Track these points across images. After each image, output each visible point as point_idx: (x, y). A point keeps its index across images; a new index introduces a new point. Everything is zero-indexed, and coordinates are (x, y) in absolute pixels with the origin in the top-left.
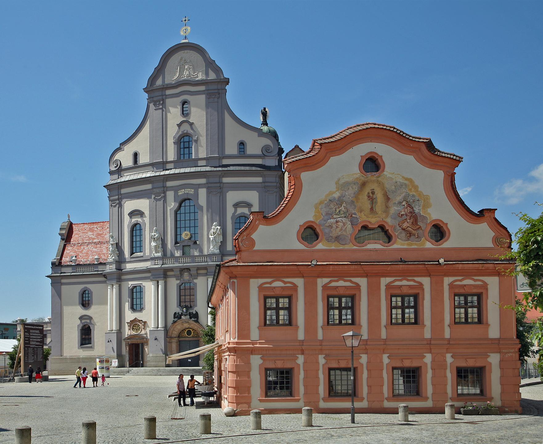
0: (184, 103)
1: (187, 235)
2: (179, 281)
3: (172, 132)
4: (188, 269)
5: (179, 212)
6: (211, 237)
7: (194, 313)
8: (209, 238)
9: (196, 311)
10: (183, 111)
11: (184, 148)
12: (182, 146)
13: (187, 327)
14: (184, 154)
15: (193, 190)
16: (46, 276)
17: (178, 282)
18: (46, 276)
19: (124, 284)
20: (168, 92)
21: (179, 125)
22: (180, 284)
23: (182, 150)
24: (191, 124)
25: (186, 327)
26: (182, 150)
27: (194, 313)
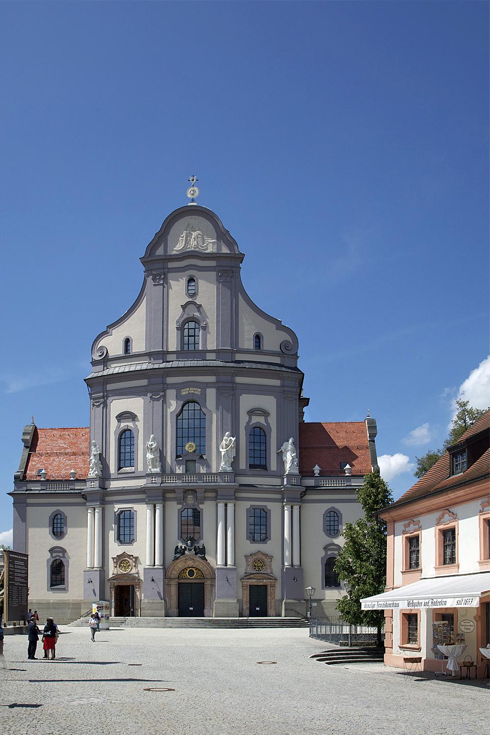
2: (181, 506)
3: (175, 314)
4: (194, 491)
5: (180, 417)
6: (223, 451)
8: (219, 453)
10: (188, 290)
11: (189, 336)
13: (190, 566)
14: (188, 344)
15: (199, 390)
17: (180, 506)
21: (184, 307)
27: (201, 547)
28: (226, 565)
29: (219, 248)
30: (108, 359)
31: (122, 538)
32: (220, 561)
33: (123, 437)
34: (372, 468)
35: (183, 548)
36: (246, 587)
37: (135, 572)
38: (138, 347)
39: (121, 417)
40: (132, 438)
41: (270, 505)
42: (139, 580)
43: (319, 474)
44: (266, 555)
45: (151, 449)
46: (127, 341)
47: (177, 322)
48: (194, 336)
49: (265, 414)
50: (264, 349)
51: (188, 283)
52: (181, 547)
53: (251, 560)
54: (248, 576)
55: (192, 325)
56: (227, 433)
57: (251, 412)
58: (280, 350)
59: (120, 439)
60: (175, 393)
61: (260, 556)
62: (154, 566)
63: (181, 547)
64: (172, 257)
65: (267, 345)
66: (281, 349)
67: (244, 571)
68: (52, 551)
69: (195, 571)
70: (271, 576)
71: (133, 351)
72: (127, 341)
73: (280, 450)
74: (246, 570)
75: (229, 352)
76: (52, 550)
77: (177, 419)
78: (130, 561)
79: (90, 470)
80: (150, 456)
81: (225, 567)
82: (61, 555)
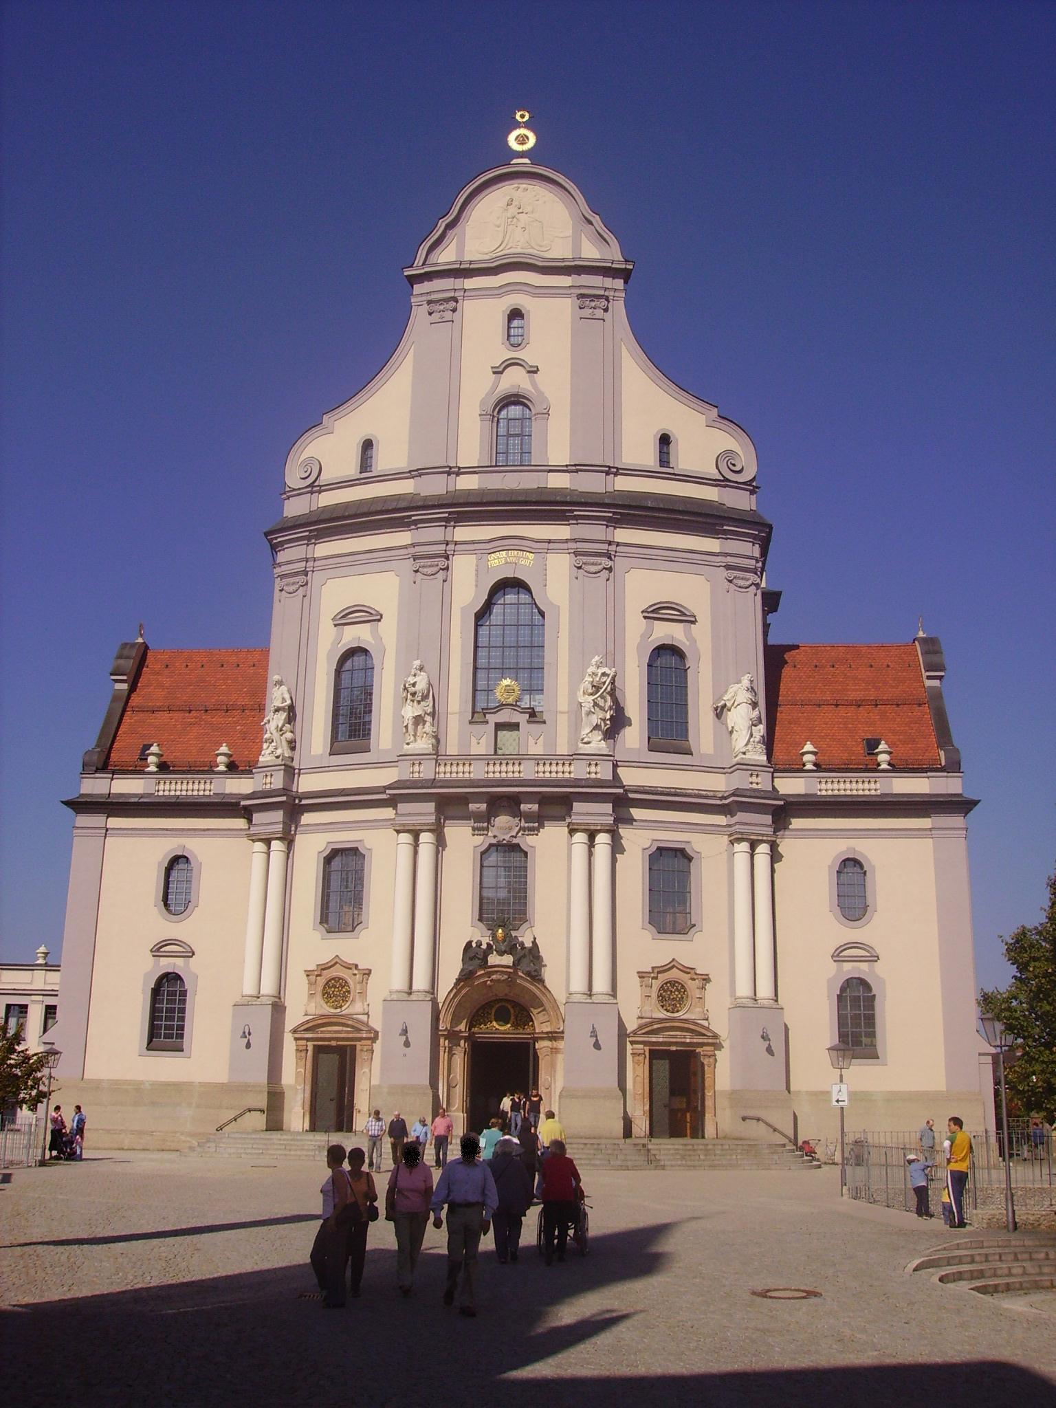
0: (515, 314)
1: (508, 690)
7: (528, 944)
9: (537, 941)
10: (509, 336)
11: (509, 435)
12: (502, 431)
13: (501, 996)
15: (531, 556)
16: (62, 802)
18: (62, 802)
19: (301, 840)
20: (470, 283)
21: (498, 372)
22: (483, 849)
23: (502, 440)
24: (534, 371)
25: (496, 995)
26: (502, 440)
27: (528, 944)
28: (590, 995)
29: (577, 245)
30: (321, 486)
31: (332, 918)
32: (578, 984)
33: (348, 665)
34: (942, 753)
35: (484, 946)
36: (641, 1058)
37: (361, 1010)
38: (387, 459)
39: (345, 618)
40: (369, 669)
41: (698, 843)
42: (371, 1030)
43: (815, 765)
44: (687, 970)
45: (414, 694)
46: (368, 445)
47: (482, 403)
48: (521, 435)
49: (685, 617)
50: (680, 467)
51: (509, 321)
52: (479, 944)
53: (656, 984)
54: (650, 1027)
55: (514, 411)
56: (597, 658)
57: (655, 613)
58: (717, 471)
59: (338, 672)
60: (475, 561)
61: (674, 974)
62: (410, 994)
63: (479, 944)
64: (472, 266)
65: (686, 458)
66: (717, 467)
67: (637, 1013)
68: (158, 950)
69: (512, 1011)
70: (703, 1027)
71: (379, 469)
72: (368, 445)
73: (723, 702)
74: (641, 1008)
75: (602, 472)
76: (158, 950)
77: (477, 626)
78: (351, 982)
79: (265, 746)
80: (410, 711)
81: (590, 1001)
82: (179, 962)
